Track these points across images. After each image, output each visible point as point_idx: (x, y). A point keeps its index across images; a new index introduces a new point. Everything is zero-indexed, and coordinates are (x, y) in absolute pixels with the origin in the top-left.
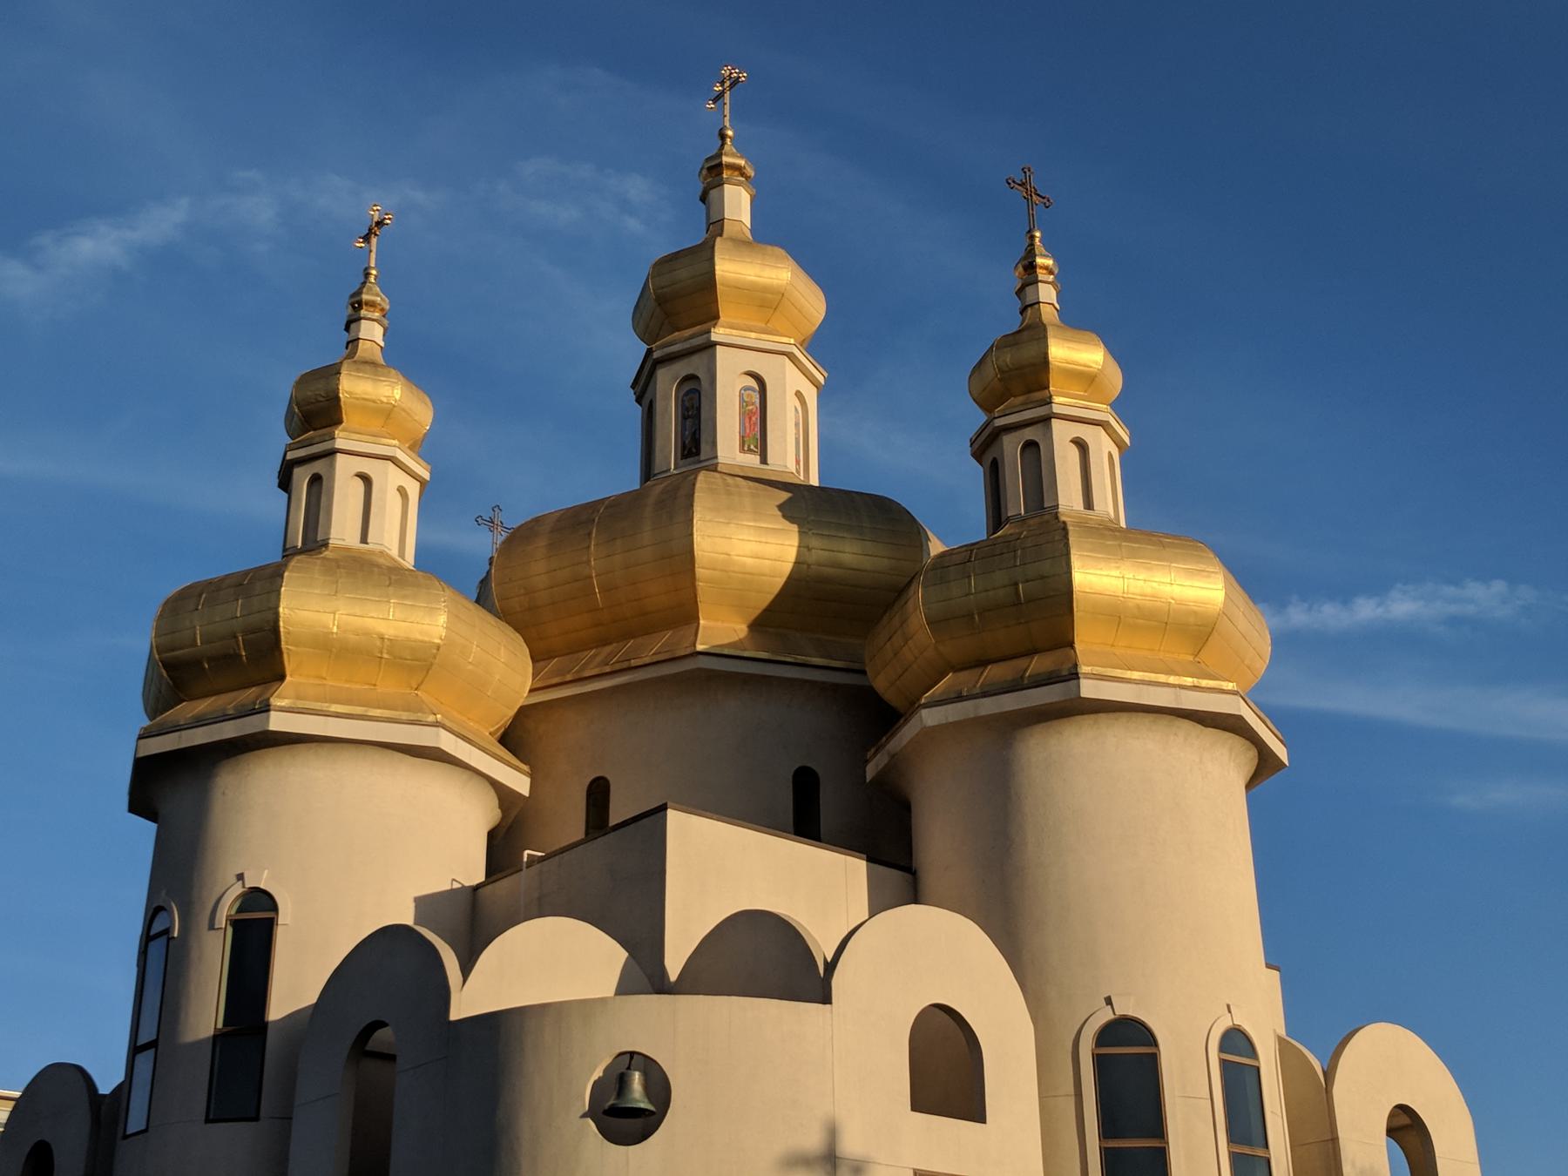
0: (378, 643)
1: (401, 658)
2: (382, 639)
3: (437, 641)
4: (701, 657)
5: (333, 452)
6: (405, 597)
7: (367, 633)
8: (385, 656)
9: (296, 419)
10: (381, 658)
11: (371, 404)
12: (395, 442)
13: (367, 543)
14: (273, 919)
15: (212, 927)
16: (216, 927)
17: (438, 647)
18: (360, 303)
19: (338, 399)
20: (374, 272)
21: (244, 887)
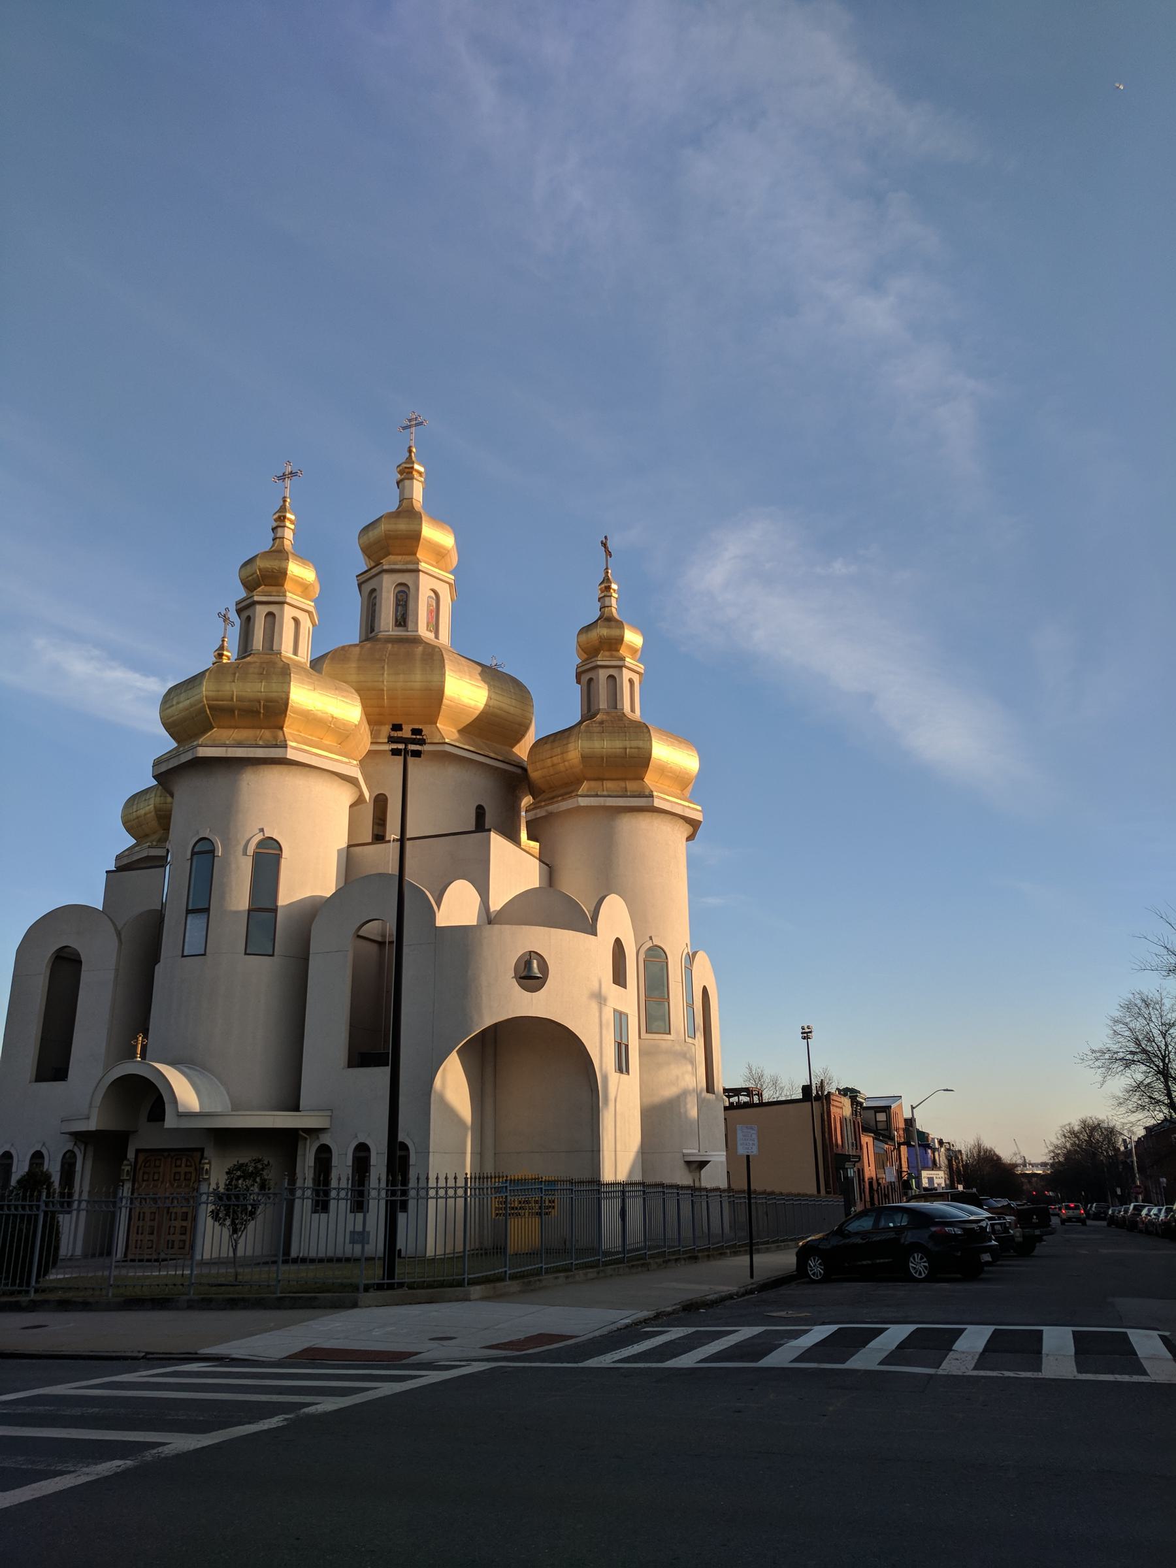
0: (330, 719)
1: (338, 728)
2: (333, 717)
3: (357, 723)
4: (446, 745)
5: (283, 603)
6: (342, 696)
7: (327, 713)
8: (332, 726)
9: (255, 576)
10: (330, 727)
11: (300, 579)
12: (313, 604)
13: (297, 656)
14: (279, 854)
15: (245, 853)
16: (248, 854)
17: (356, 726)
18: (285, 517)
19: (287, 574)
20: (288, 500)
21: (264, 836)
